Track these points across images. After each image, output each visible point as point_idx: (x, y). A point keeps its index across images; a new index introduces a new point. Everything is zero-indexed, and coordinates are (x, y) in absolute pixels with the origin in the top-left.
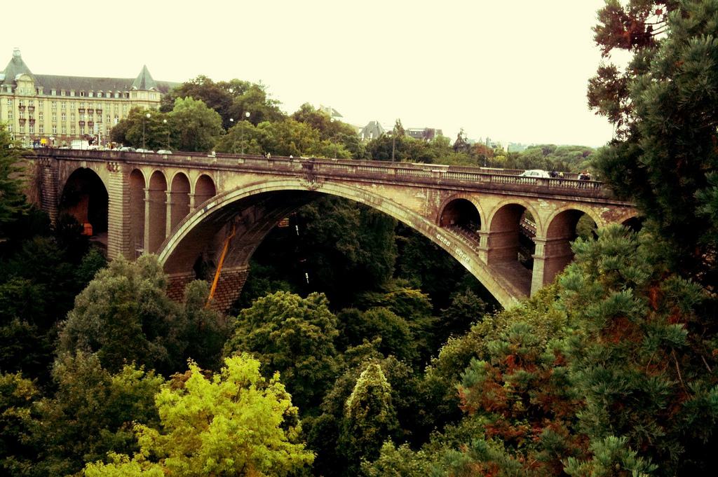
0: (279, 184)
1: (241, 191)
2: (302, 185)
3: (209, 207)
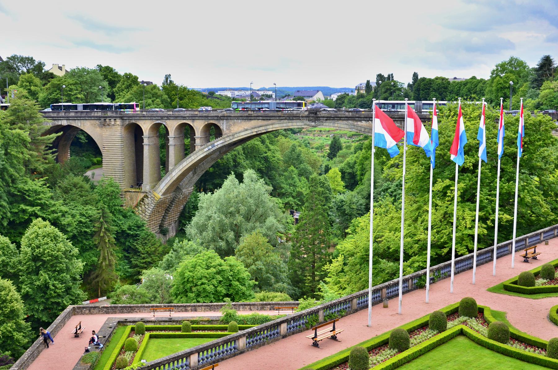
0: (285, 125)
1: (249, 132)
2: (305, 125)
3: (216, 144)
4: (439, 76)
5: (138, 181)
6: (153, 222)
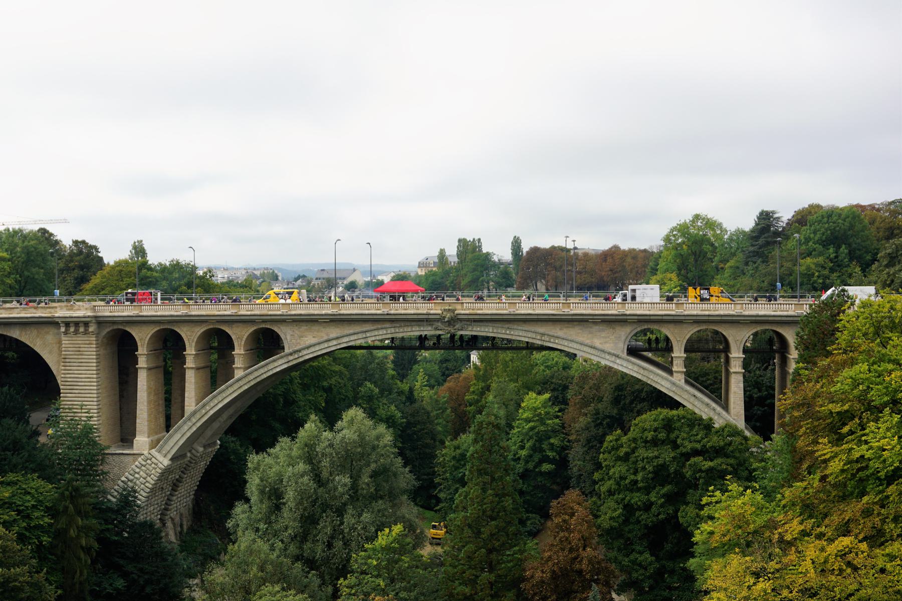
4: (556, 245)
5: (126, 436)
6: (152, 508)
